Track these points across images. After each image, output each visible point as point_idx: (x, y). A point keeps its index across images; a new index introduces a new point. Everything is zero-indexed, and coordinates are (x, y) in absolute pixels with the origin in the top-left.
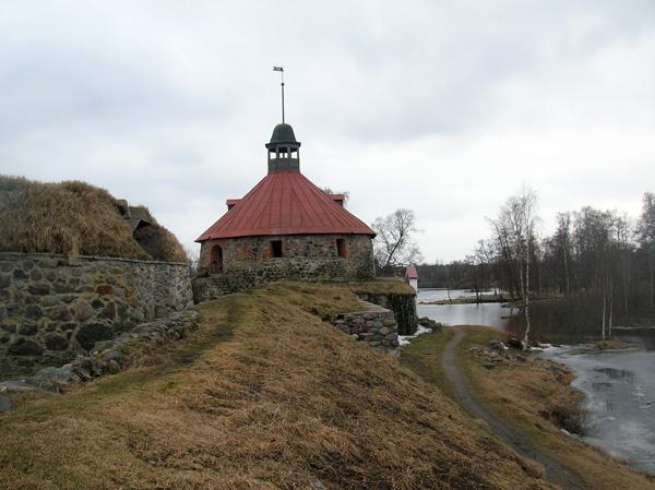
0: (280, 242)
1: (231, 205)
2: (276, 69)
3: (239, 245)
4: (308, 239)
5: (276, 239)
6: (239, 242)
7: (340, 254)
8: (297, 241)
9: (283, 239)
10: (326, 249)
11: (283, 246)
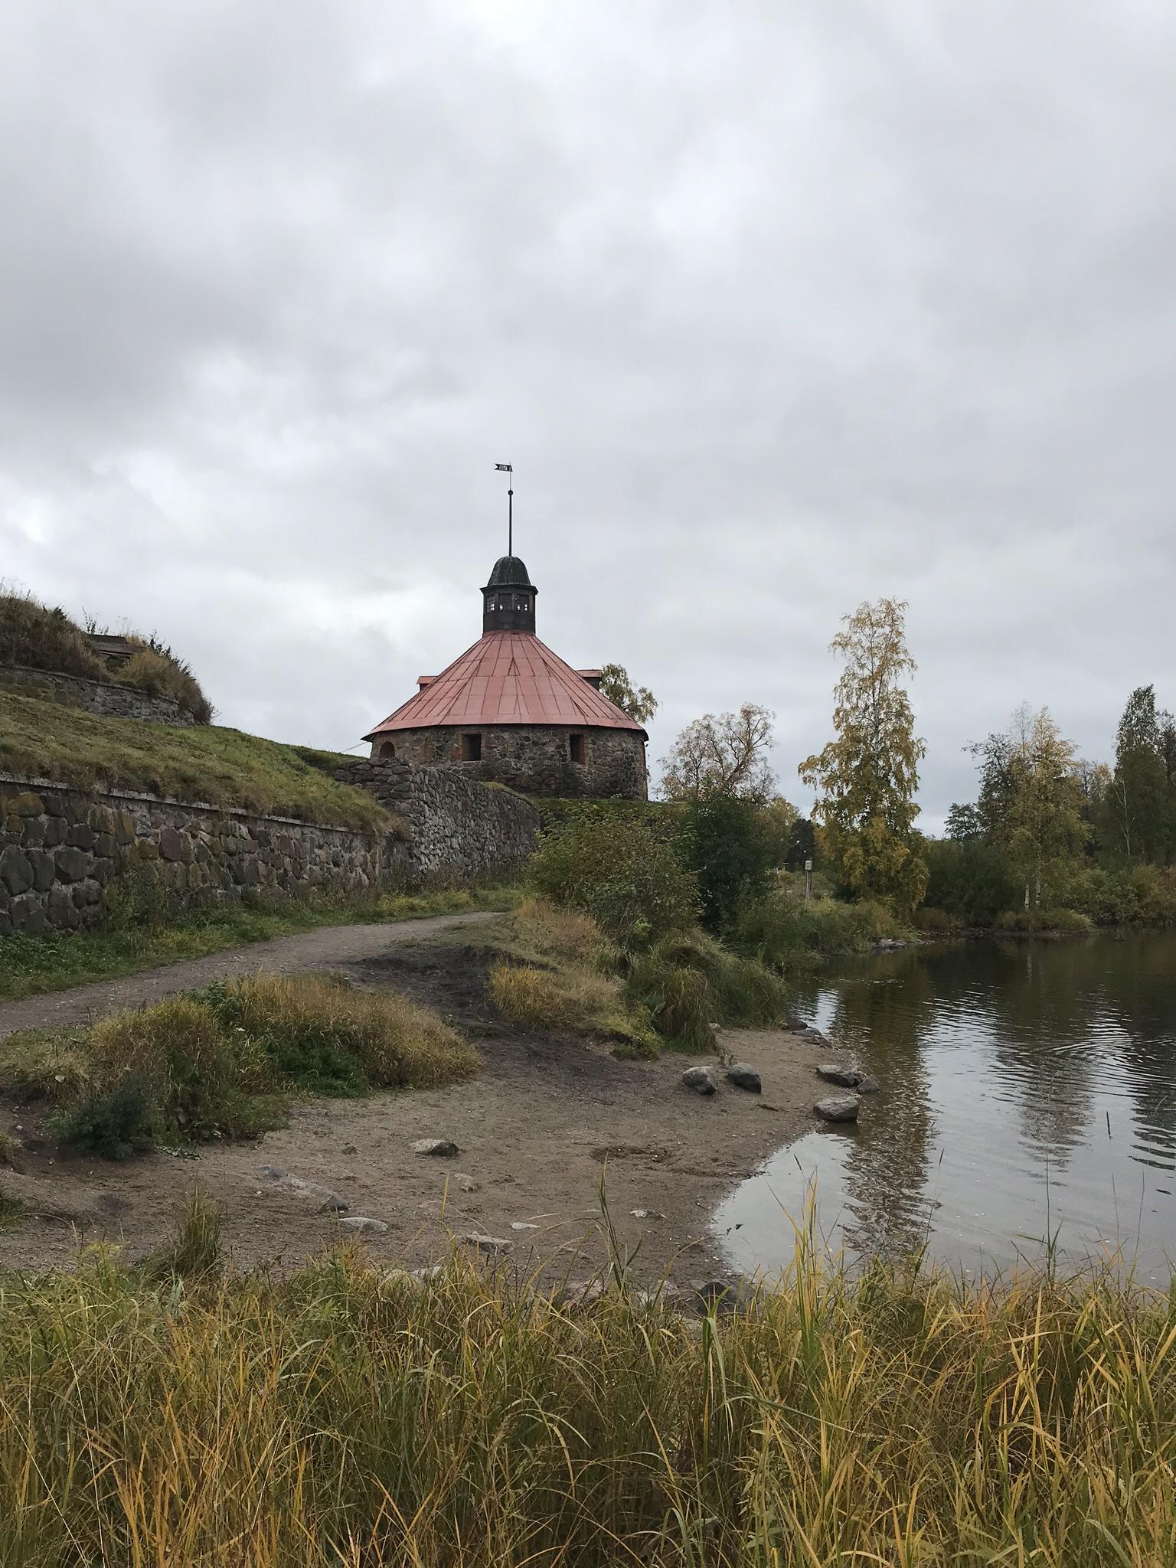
0: (478, 737)
2: (499, 467)
3: (418, 741)
4: (524, 733)
5: (474, 732)
8: (506, 735)
9: (484, 734)
10: (551, 749)
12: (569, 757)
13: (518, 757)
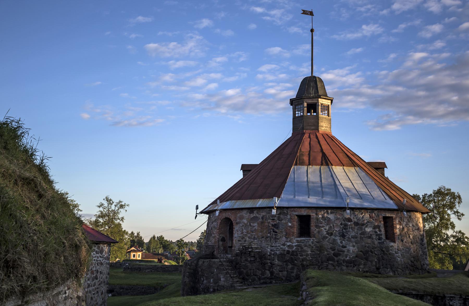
0: (309, 217)
1: (246, 168)
2: (305, 12)
3: (255, 219)
6: (255, 214)
7: (387, 238)
9: (313, 215)
11: (313, 224)
12: (383, 237)
13: (343, 236)
